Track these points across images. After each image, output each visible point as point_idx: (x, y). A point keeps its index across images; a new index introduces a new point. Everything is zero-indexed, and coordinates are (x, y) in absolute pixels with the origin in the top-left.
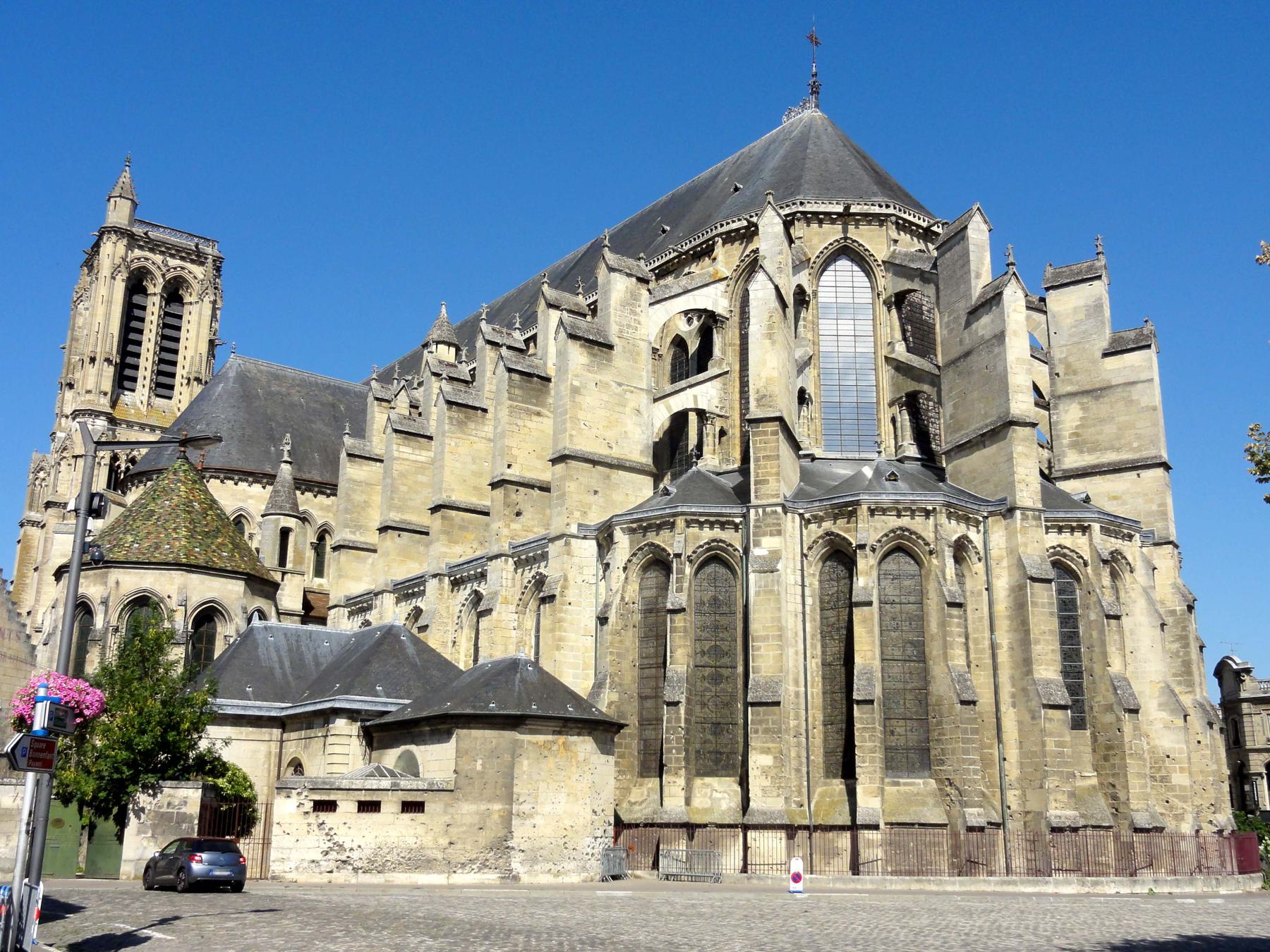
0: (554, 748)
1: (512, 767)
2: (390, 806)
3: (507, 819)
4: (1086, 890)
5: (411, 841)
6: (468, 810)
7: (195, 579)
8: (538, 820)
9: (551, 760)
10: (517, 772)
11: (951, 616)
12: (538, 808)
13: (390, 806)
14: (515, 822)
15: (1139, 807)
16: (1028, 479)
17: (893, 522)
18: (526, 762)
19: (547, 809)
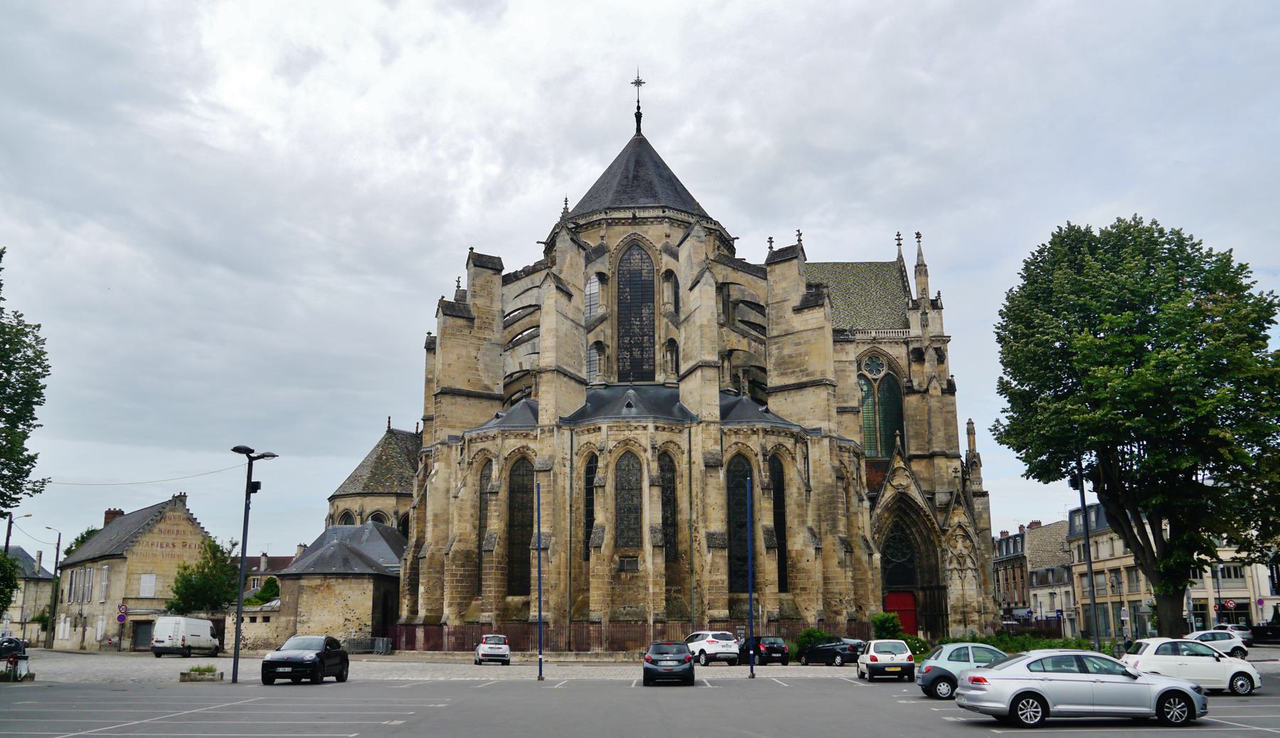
0: (322, 588)
1: (298, 599)
2: (259, 620)
3: (295, 623)
4: (526, 659)
5: (265, 635)
6: (283, 619)
7: (368, 500)
8: (311, 624)
9: (320, 595)
10: (300, 601)
11: (491, 500)
12: (312, 618)
13: (259, 620)
14: (298, 625)
15: (596, 608)
16: (547, 407)
17: (481, 446)
18: (305, 596)
19: (317, 618)
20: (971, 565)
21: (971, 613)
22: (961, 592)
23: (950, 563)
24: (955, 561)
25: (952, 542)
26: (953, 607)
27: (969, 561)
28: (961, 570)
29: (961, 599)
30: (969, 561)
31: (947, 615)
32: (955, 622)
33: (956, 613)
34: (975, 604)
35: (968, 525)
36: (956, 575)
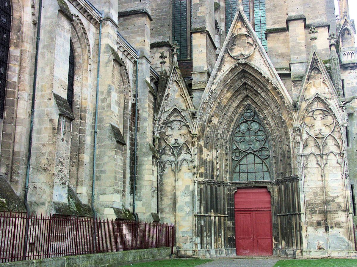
20: (334, 149)
21: (336, 212)
22: (320, 184)
23: (305, 146)
24: (311, 144)
25: (308, 120)
26: (308, 204)
27: (331, 143)
28: (321, 156)
29: (320, 193)
30: (331, 143)
31: (300, 214)
32: (311, 224)
33: (312, 212)
34: (340, 200)
35: (329, 96)
36: (313, 163)
